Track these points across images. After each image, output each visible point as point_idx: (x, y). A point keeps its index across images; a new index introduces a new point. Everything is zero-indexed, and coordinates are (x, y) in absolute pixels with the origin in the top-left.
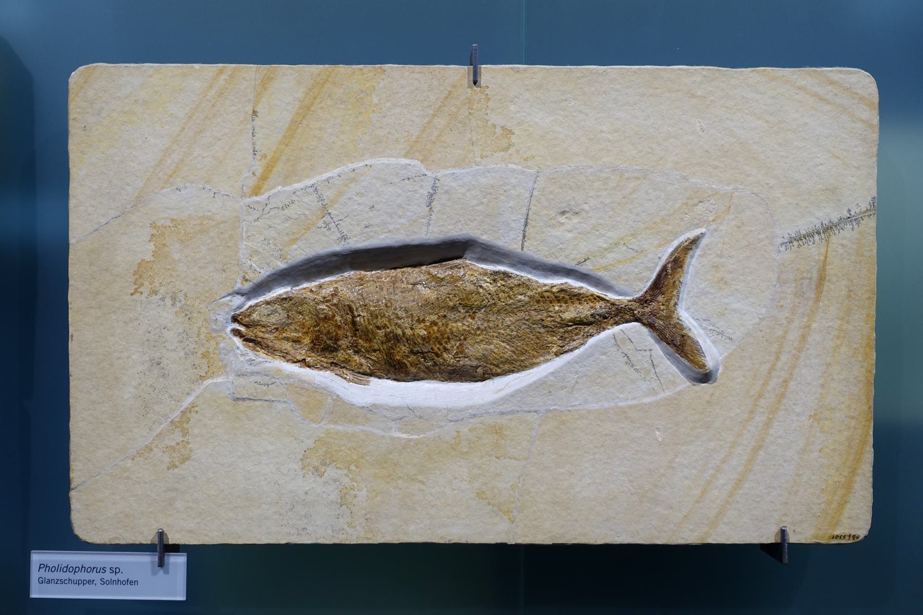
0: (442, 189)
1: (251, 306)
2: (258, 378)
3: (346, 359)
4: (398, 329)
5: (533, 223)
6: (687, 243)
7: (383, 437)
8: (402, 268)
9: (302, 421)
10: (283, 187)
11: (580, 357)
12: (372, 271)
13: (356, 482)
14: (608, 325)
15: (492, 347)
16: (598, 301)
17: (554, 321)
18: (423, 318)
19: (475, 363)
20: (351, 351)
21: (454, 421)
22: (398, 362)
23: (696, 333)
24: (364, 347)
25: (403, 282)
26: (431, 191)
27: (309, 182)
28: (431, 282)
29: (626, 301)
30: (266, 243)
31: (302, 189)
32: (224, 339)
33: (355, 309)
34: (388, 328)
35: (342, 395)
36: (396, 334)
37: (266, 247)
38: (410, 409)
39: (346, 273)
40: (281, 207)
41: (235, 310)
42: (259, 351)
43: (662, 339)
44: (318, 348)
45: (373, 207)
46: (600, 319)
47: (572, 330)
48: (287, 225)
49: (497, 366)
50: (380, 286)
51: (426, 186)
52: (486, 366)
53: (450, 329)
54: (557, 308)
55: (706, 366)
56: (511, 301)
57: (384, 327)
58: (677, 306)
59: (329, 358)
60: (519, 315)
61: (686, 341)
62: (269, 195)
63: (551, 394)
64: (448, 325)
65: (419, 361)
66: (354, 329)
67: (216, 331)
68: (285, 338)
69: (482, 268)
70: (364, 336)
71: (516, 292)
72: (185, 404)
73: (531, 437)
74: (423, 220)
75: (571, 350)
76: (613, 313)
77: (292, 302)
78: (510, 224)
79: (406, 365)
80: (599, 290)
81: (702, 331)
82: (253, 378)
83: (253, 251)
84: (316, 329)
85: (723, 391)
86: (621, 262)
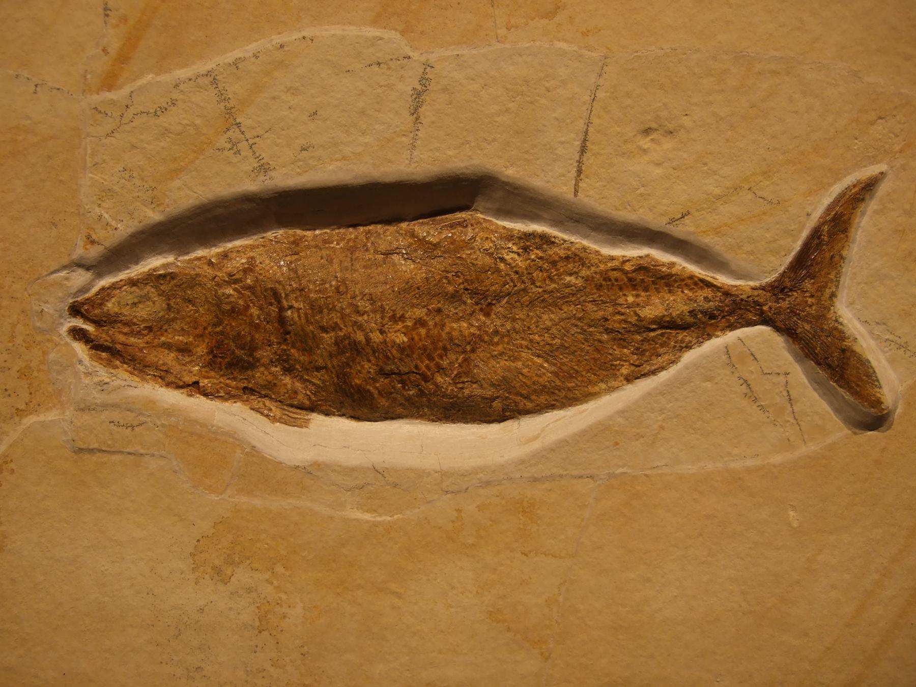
0: (438, 83)
1: (103, 289)
2: (116, 415)
3: (270, 382)
4: (358, 332)
5: (595, 148)
6: (857, 189)
7: (331, 518)
8: (366, 225)
9: (193, 490)
10: (157, 74)
11: (668, 385)
12: (315, 230)
13: (286, 593)
14: (716, 330)
15: (519, 364)
16: (702, 288)
17: (625, 321)
18: (401, 313)
19: (490, 393)
20: (278, 369)
21: (453, 492)
22: (359, 390)
23: (864, 346)
24: (300, 362)
25: (367, 250)
26: (419, 87)
27: (202, 67)
28: (416, 250)
29: (748, 289)
30: (127, 176)
31: (190, 80)
32: (56, 345)
33: (283, 295)
34: (341, 329)
35: (259, 446)
36: (355, 341)
37: (127, 183)
39: (269, 233)
40: (152, 111)
41: (76, 294)
42: (118, 368)
43: (807, 356)
44: (220, 363)
45: (315, 113)
46: (704, 319)
47: (656, 337)
48: (162, 144)
49: (527, 397)
50: (328, 256)
51: (410, 77)
52: (507, 397)
53: (449, 333)
54: (631, 299)
55: (882, 403)
56: (553, 286)
57: (333, 329)
58: (835, 299)
59: (241, 379)
60: (566, 310)
61: (849, 359)
62: (132, 90)
63: (618, 446)
64: (443, 325)
65: (393, 387)
66: (281, 331)
67: (41, 331)
68: (164, 344)
69: (504, 228)
70: (299, 344)
71: (561, 270)
73: (583, 520)
74: (404, 139)
75: (654, 372)
76: (727, 309)
77: (175, 281)
78: (556, 149)
79: (371, 394)
80: (702, 269)
81: (872, 343)
82: (105, 415)
83: (103, 191)
84: (218, 329)
85: (902, 443)
86: (743, 220)
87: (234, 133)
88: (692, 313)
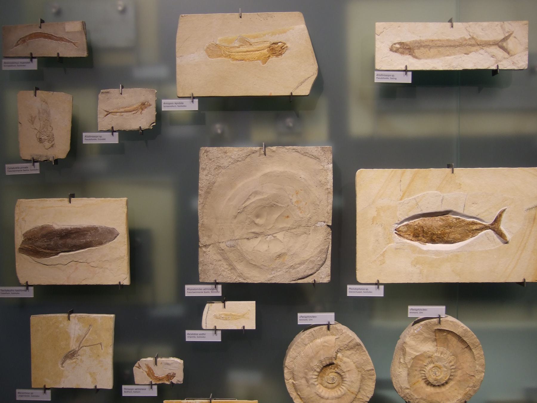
2: (401, 244)
15: (456, 236)
27: (413, 197)
38: (437, 251)
54: (471, 226)
67: (392, 233)
72: (384, 250)
75: (475, 236)
81: (506, 232)
87: (418, 206)
88: (480, 228)
